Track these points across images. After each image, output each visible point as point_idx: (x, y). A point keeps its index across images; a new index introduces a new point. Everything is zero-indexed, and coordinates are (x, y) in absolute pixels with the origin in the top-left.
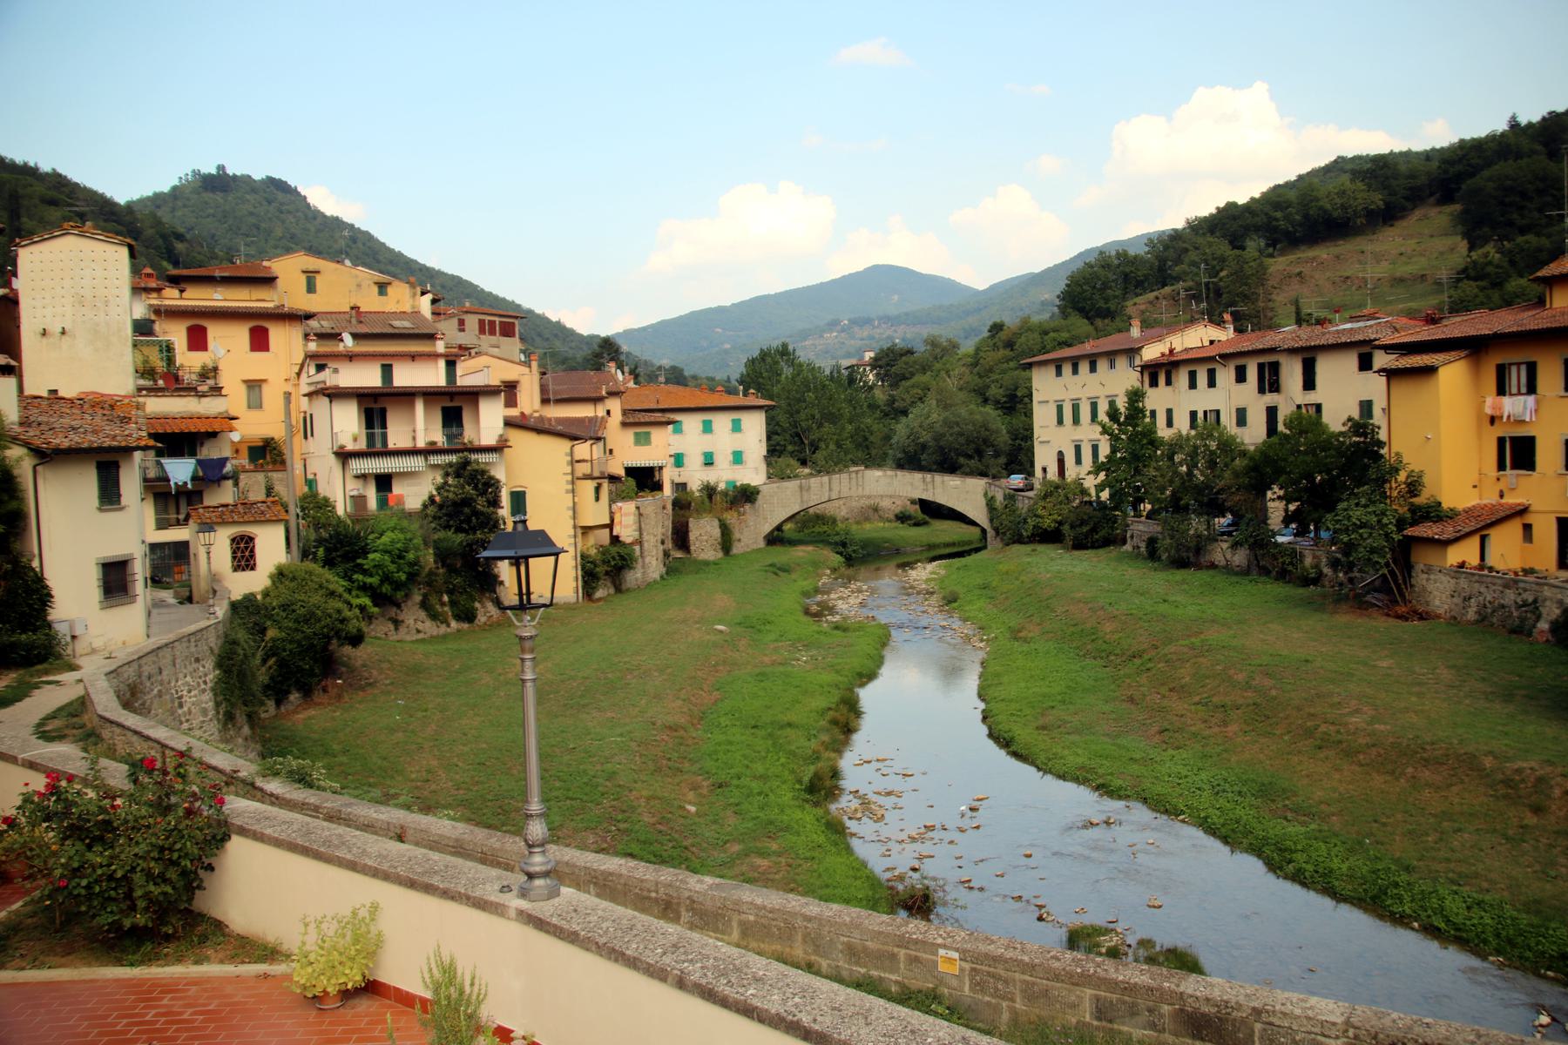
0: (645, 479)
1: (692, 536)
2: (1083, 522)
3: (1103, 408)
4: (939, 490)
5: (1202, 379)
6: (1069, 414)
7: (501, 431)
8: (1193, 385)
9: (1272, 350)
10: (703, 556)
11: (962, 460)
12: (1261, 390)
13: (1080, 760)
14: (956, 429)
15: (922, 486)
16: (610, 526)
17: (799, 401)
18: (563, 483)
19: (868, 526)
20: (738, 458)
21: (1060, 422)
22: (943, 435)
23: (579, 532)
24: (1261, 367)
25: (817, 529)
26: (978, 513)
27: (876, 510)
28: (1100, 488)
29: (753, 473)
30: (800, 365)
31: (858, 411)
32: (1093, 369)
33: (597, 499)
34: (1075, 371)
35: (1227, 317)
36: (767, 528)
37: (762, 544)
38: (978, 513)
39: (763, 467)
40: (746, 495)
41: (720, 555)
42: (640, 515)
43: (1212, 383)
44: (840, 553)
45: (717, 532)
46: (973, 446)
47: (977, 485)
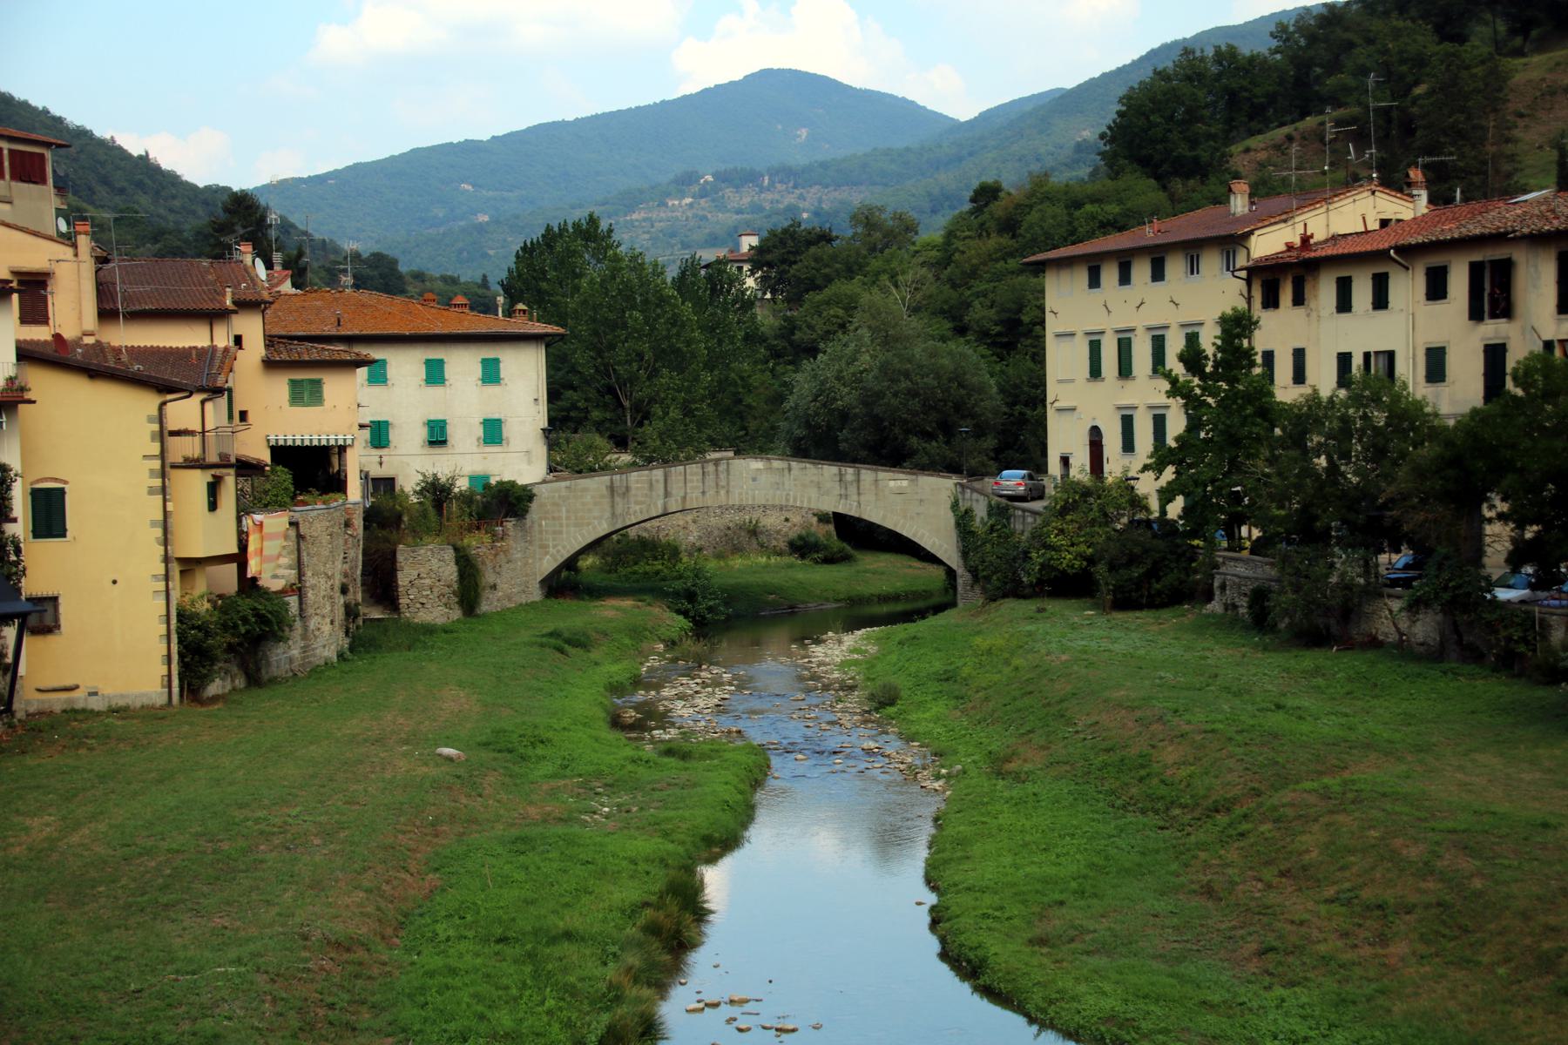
0: (311, 469)
1: (403, 579)
2: (1133, 560)
3: (1175, 345)
4: (868, 497)
5: (1362, 293)
6: (1110, 357)
7: (11, 371)
8: (1344, 305)
9: (1499, 238)
10: (424, 617)
11: (914, 441)
12: (1476, 314)
13: (1107, 1004)
14: (904, 384)
15: (837, 490)
16: (240, 559)
17: (614, 326)
18: (143, 474)
19: (737, 562)
20: (493, 432)
21: (1095, 372)
22: (879, 395)
23: (176, 569)
24: (1476, 271)
25: (642, 568)
26: (939, 537)
27: (754, 531)
28: (1166, 495)
29: (522, 461)
30: (617, 259)
31: (727, 346)
32: (1158, 275)
33: (213, 506)
34: (1125, 279)
35: (1416, 174)
36: (548, 565)
37: (536, 595)
38: (939, 537)
39: (540, 450)
40: (507, 503)
41: (456, 614)
42: (300, 537)
43: (1380, 301)
44: (685, 614)
45: (450, 571)
46: (934, 416)
47: (938, 489)
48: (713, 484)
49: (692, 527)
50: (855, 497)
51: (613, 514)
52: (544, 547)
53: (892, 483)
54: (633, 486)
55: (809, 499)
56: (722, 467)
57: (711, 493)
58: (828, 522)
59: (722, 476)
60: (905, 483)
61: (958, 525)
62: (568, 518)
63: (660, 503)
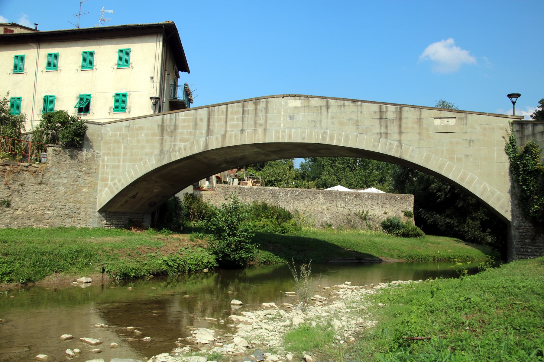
4: (411, 136)
15: (376, 127)
20: (121, 101)
36: (105, 195)
37: (94, 221)
48: (252, 122)
49: (326, 212)
50: (396, 136)
51: (162, 152)
52: (105, 179)
53: (437, 122)
54: (180, 124)
55: (347, 137)
56: (262, 105)
57: (249, 130)
58: (410, 216)
59: (261, 114)
60: (452, 122)
61: (514, 169)
62: (125, 154)
63: (202, 141)
